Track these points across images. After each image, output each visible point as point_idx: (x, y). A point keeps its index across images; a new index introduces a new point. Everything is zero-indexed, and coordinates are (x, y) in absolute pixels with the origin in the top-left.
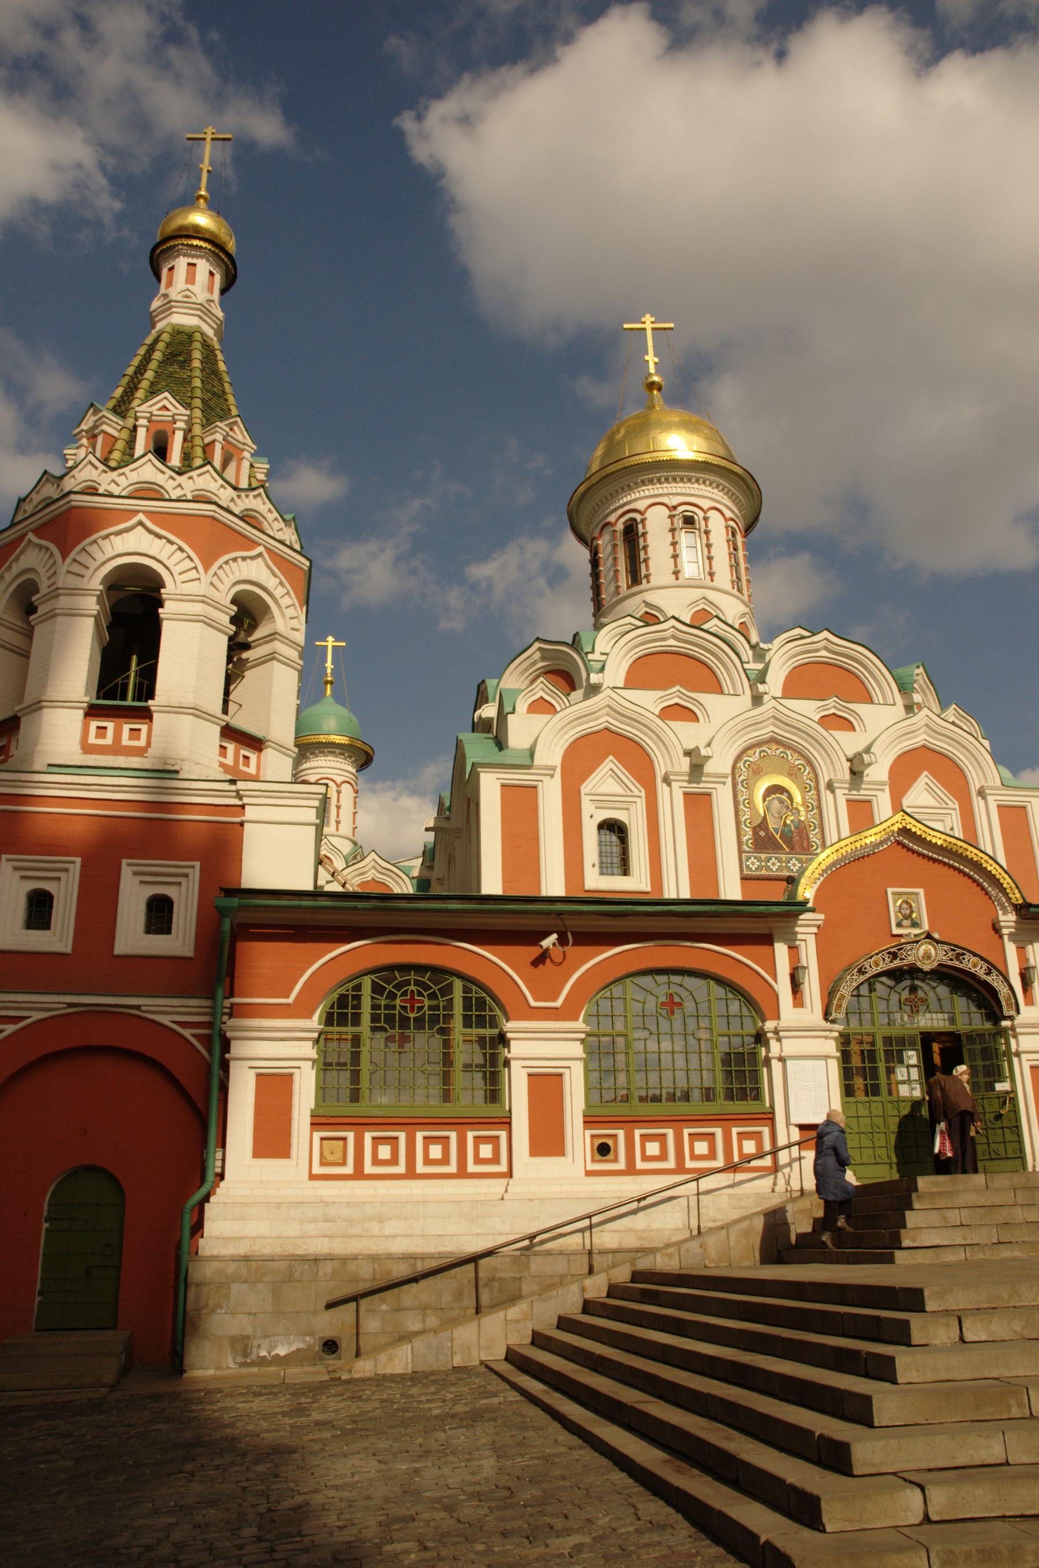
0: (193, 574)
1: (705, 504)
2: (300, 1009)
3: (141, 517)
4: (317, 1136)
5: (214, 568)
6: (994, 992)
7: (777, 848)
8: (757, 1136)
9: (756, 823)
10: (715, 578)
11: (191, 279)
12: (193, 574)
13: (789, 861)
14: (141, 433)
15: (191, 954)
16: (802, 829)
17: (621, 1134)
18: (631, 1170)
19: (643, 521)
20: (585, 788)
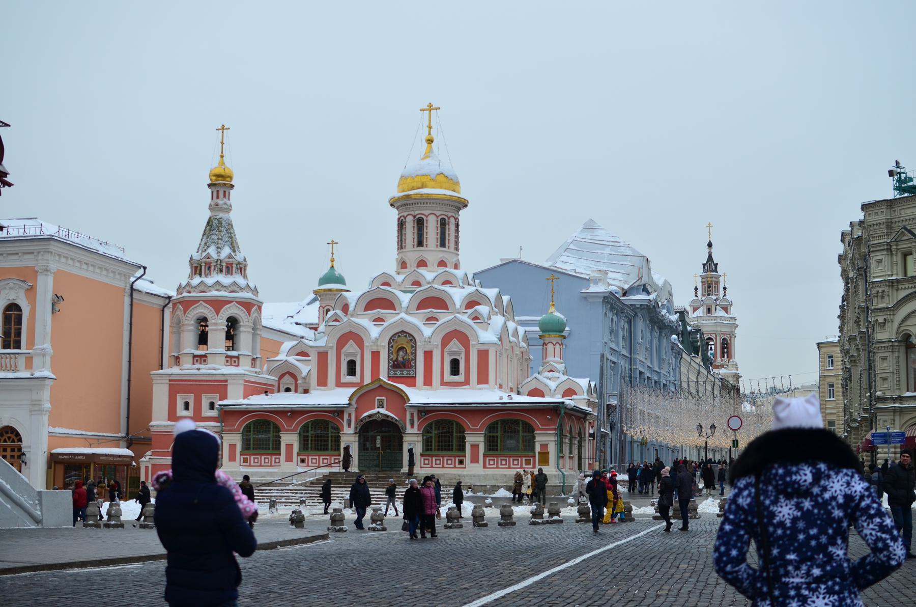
0: (214, 318)
1: (427, 213)
2: (237, 430)
3: (201, 302)
4: (242, 457)
5: (220, 314)
6: (398, 426)
7: (400, 368)
8: (339, 459)
9: (394, 359)
10: (428, 246)
11: (218, 197)
12: (214, 318)
13: (403, 371)
14: (203, 268)
15: (217, 416)
16: (409, 361)
17: (306, 457)
18: (308, 466)
19: (405, 222)
20: (343, 351)
